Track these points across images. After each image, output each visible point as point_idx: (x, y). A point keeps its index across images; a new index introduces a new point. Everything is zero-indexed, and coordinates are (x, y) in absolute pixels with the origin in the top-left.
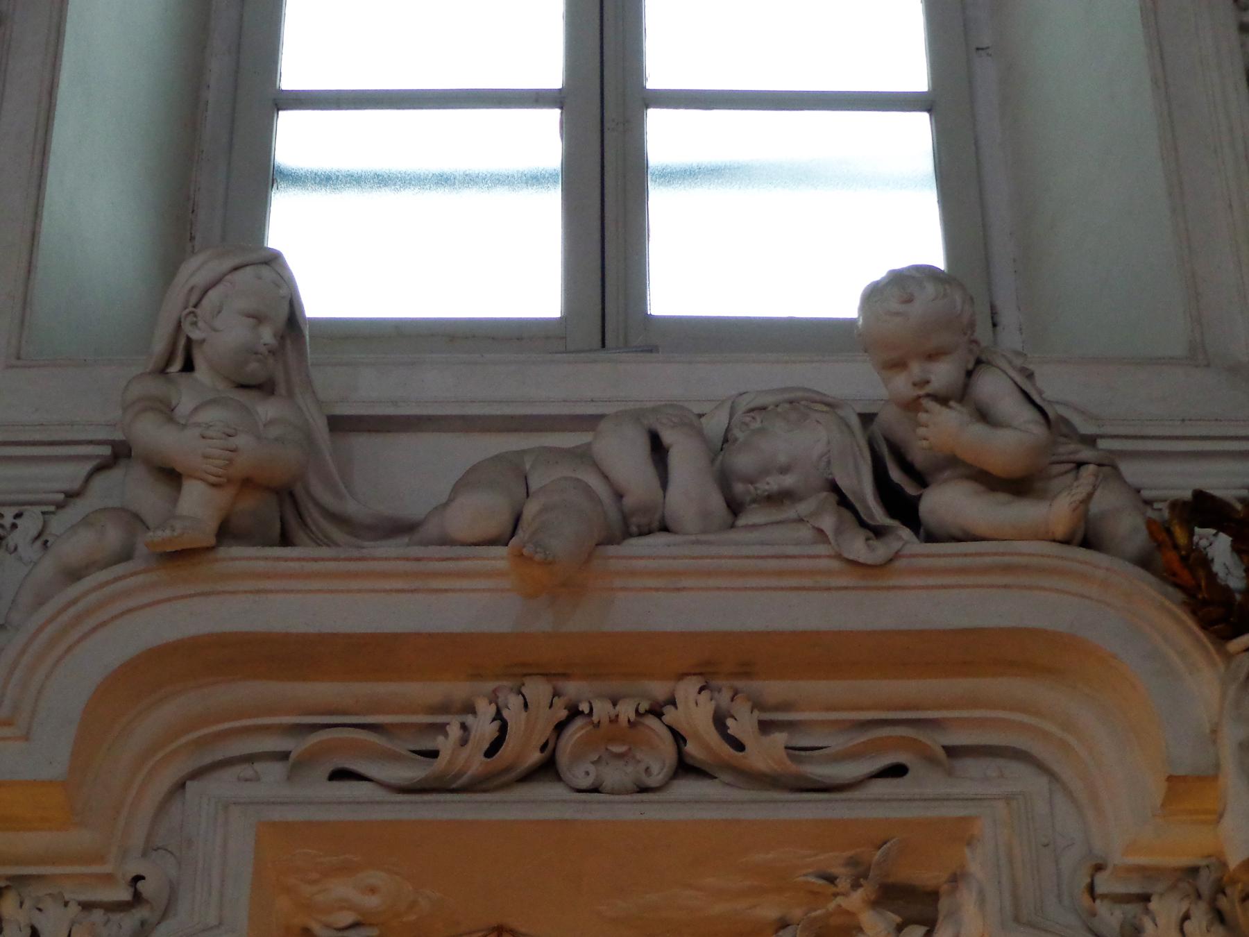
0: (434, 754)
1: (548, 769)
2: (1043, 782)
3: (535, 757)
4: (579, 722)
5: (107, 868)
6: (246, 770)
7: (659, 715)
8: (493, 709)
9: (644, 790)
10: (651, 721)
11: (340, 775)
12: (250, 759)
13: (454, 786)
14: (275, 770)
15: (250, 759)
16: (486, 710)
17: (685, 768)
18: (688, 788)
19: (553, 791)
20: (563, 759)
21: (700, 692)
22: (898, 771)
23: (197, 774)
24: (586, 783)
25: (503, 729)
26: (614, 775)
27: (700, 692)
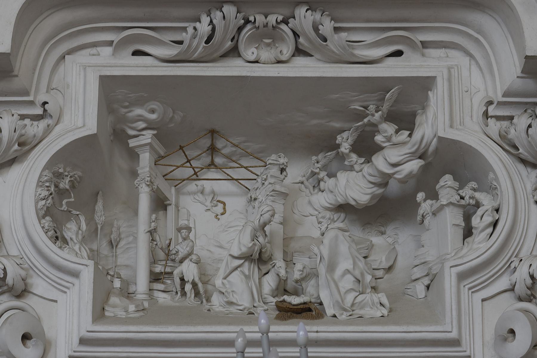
0: (180, 43)
1: (234, 52)
2: (467, 59)
3: (229, 44)
4: (249, 26)
5: (31, 98)
6: (94, 51)
7: (287, 23)
8: (208, 19)
9: (279, 62)
10: (284, 27)
11: (137, 53)
12: (94, 45)
13: (191, 59)
14: (108, 50)
15: (94, 45)
16: (205, 20)
17: (299, 52)
18: (300, 61)
19: (238, 62)
20: (241, 47)
21: (306, 12)
22: (398, 53)
23: (70, 52)
24: (252, 58)
25: (214, 29)
26: (265, 54)
27: (306, 12)
